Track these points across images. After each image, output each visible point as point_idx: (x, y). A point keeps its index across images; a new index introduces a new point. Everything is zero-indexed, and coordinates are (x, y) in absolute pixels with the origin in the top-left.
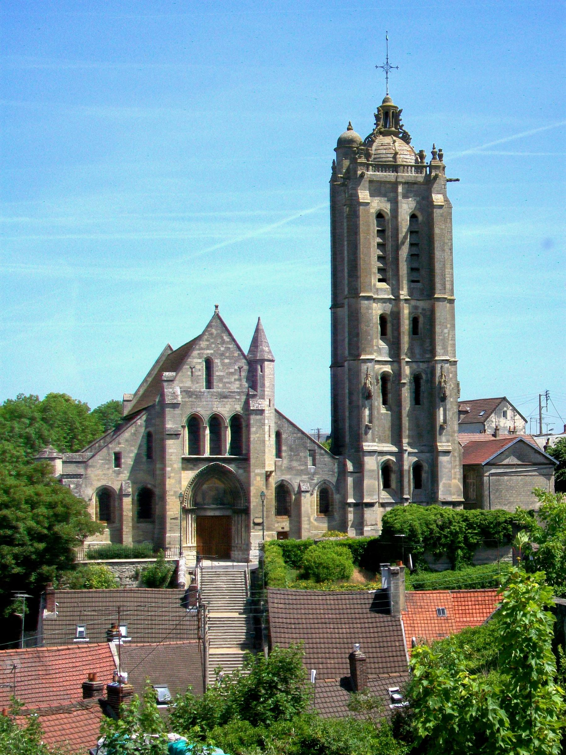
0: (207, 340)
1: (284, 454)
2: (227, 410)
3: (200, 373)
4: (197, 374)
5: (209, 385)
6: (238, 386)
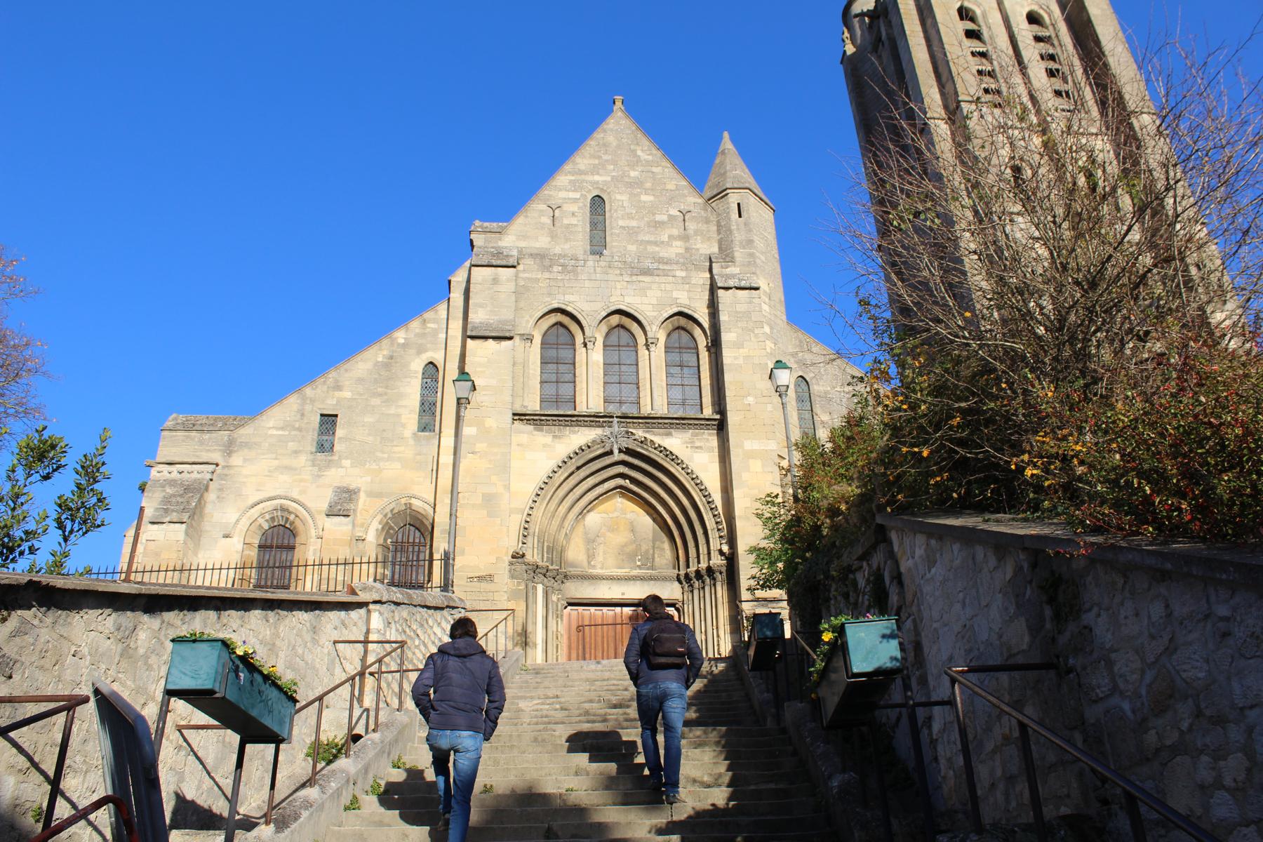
2: (652, 303)
3: (574, 221)
4: (566, 222)
5: (598, 245)
6: (682, 251)
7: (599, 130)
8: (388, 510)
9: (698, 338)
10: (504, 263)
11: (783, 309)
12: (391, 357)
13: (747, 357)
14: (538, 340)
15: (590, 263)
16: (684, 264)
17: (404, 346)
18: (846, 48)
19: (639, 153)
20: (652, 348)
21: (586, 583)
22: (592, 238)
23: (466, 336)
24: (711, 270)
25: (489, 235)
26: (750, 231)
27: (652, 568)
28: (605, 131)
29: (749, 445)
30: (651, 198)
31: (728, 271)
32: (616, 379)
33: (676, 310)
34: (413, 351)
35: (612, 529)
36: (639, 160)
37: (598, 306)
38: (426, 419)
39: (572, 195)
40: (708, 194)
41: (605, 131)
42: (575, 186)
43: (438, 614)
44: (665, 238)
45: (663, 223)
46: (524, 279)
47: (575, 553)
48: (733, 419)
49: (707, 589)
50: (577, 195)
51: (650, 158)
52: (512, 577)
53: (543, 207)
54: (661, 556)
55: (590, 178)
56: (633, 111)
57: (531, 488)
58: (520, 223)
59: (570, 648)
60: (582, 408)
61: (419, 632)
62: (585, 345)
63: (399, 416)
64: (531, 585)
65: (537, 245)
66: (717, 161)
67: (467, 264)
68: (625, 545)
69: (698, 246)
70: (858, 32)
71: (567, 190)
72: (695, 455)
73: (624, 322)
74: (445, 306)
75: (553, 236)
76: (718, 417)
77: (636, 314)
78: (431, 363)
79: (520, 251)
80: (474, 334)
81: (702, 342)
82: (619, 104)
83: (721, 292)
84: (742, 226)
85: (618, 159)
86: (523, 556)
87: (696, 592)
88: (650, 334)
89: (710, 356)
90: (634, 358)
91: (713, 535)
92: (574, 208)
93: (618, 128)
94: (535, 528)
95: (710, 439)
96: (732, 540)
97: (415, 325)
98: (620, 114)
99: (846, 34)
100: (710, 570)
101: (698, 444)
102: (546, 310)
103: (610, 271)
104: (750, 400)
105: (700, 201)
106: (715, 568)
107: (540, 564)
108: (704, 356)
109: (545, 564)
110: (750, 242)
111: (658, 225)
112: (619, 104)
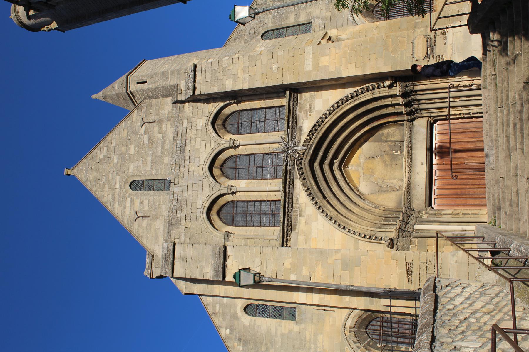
0: (103, 190)
1: (303, 19)
2: (205, 143)
3: (146, 202)
4: (146, 208)
5: (164, 185)
6: (169, 124)
7: (85, 185)
8: (354, 346)
9: (231, 108)
10: (171, 252)
11: (214, 50)
12: (240, 339)
13: (244, 72)
14: (229, 229)
15: (176, 190)
16: (178, 122)
17: (231, 329)
18: (53, 28)
19: (102, 156)
20: (237, 143)
21: (413, 192)
22: (159, 190)
23: (223, 282)
24: (183, 102)
25: (154, 265)
26: (156, 74)
27: (402, 142)
28: (86, 181)
29: (308, 66)
30: (132, 147)
31: (183, 88)
32: (259, 171)
33: (210, 127)
34: (236, 323)
35: (372, 173)
36: (107, 156)
37: (206, 184)
38: (286, 314)
39: (128, 204)
40: (132, 107)
41: (86, 181)
42: (123, 201)
43: (442, 300)
44: (160, 136)
45: (150, 138)
46: (185, 238)
47: (390, 201)
48: (288, 80)
49: (419, 97)
50: (129, 200)
51: (105, 148)
52: (408, 248)
53: (136, 224)
54: (393, 136)
55: (117, 191)
56: (74, 162)
57: (339, 234)
58: (146, 242)
59: (465, 205)
60: (279, 196)
61: (462, 317)
62: (234, 193)
63: (283, 335)
64: (414, 234)
65: (162, 229)
66: (111, 102)
67: (173, 280)
68: (385, 163)
69: (166, 112)
70: (43, 19)
71: (124, 206)
72: (316, 107)
73: (220, 165)
74: (204, 298)
75: (156, 217)
76: (288, 92)
77: (212, 156)
78: (245, 309)
79: (165, 241)
80: (221, 276)
81: (234, 107)
82: (69, 172)
83: (197, 93)
84: (153, 80)
85: (105, 172)
86: (391, 239)
87: (422, 107)
88: (227, 145)
89: (244, 101)
90: (245, 158)
91: (377, 93)
92: (137, 202)
93: (85, 172)
94: (369, 230)
95: (305, 98)
96: (379, 78)
97: (217, 321)
98: (75, 170)
99: (45, 28)
100: (405, 95)
101: (308, 107)
102: (208, 222)
103: (181, 175)
104: (274, 67)
105: (135, 112)
106: (403, 90)
107: (398, 226)
108: (245, 105)
109: (398, 223)
110: (164, 74)
111: (151, 141)
112: (69, 172)
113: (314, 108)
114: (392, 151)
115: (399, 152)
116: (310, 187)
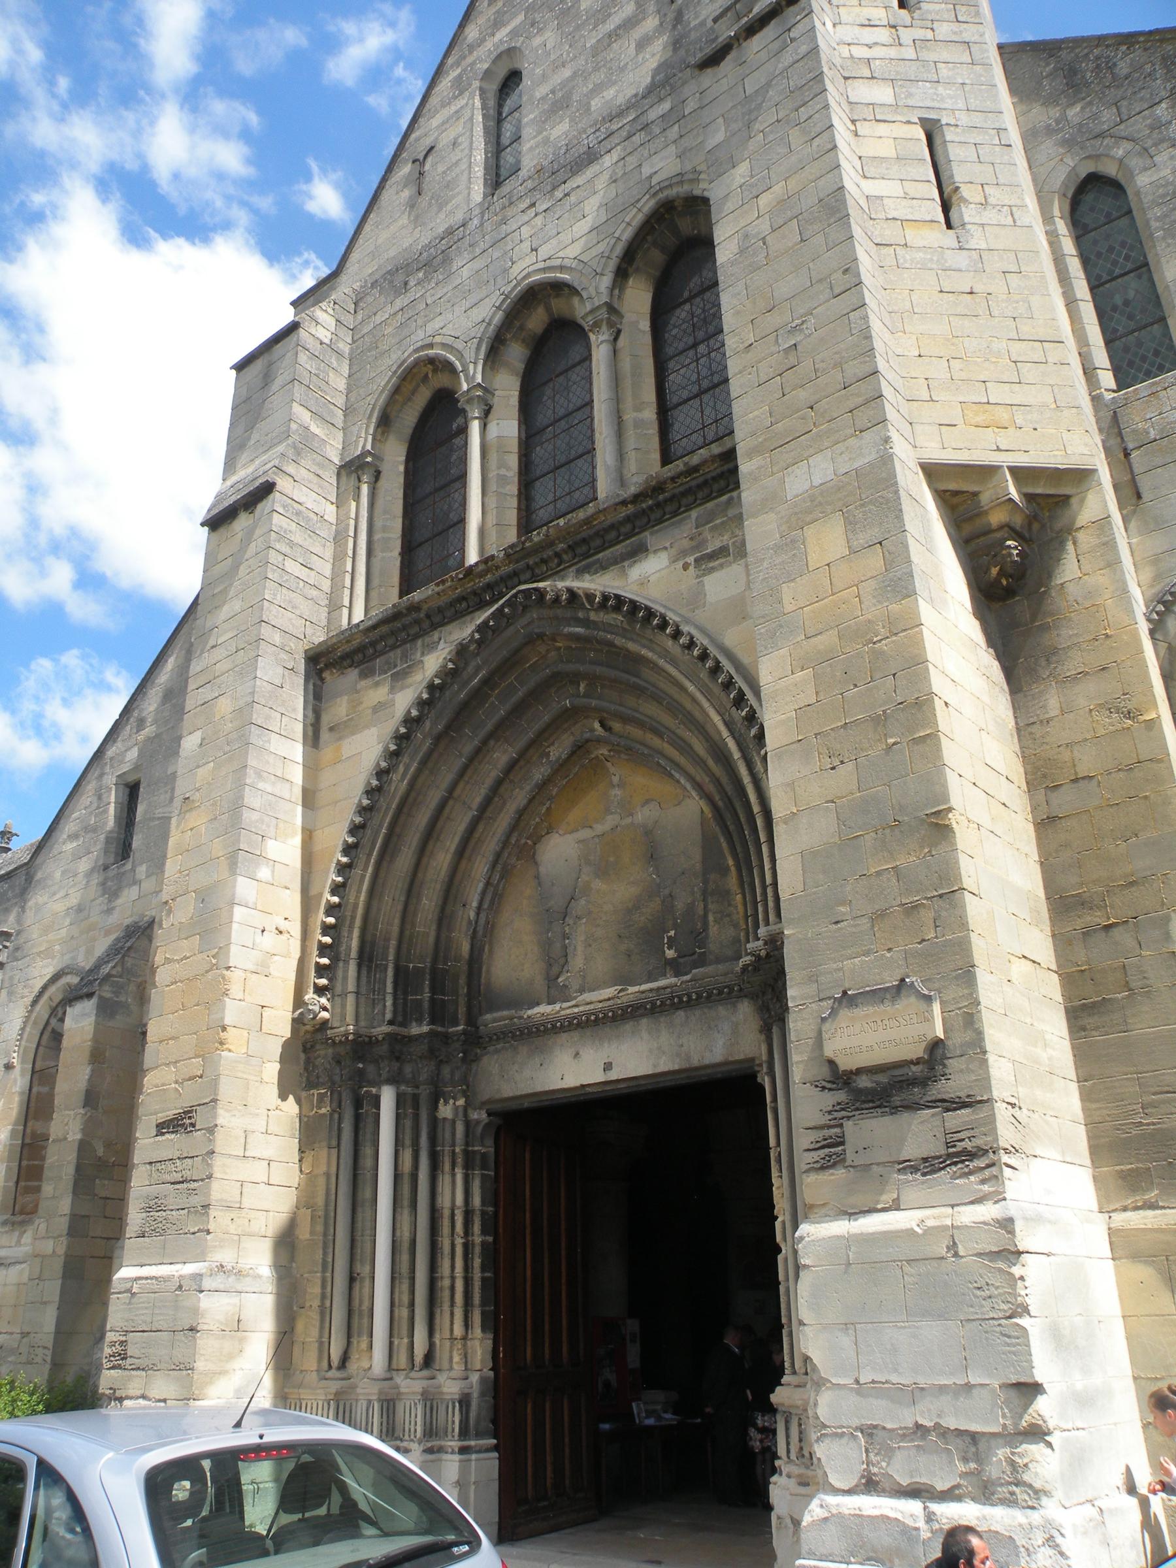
35: (604, 870)
113: (713, 569)
114: (675, 926)
115: (670, 954)
116: (465, 675)
